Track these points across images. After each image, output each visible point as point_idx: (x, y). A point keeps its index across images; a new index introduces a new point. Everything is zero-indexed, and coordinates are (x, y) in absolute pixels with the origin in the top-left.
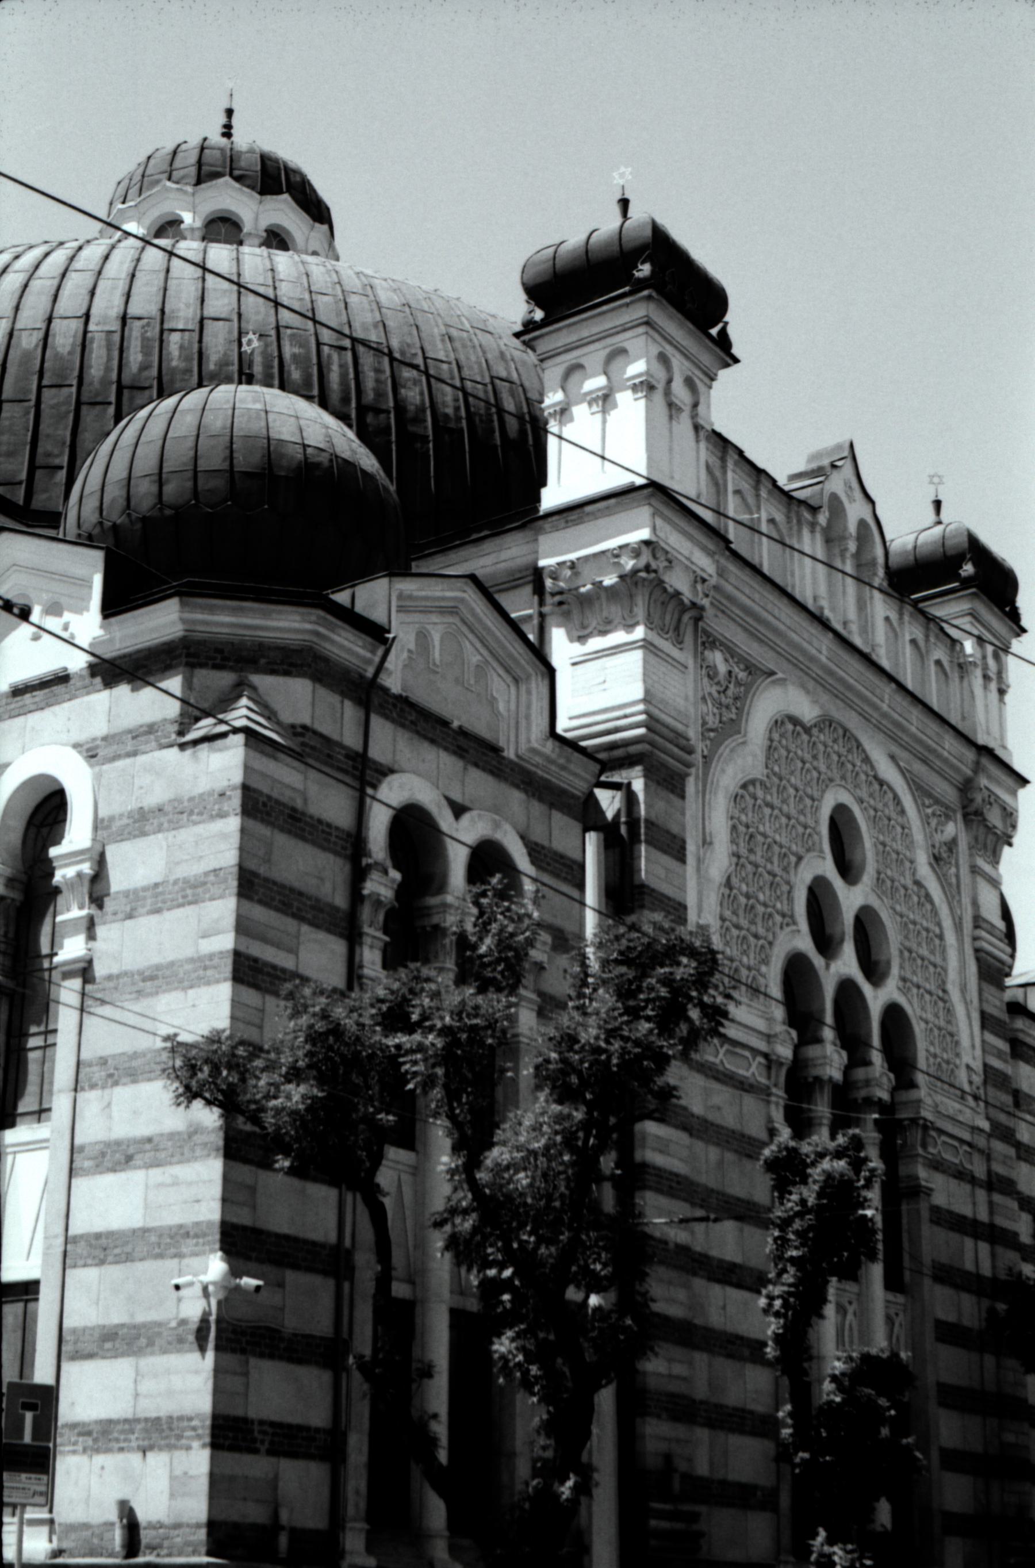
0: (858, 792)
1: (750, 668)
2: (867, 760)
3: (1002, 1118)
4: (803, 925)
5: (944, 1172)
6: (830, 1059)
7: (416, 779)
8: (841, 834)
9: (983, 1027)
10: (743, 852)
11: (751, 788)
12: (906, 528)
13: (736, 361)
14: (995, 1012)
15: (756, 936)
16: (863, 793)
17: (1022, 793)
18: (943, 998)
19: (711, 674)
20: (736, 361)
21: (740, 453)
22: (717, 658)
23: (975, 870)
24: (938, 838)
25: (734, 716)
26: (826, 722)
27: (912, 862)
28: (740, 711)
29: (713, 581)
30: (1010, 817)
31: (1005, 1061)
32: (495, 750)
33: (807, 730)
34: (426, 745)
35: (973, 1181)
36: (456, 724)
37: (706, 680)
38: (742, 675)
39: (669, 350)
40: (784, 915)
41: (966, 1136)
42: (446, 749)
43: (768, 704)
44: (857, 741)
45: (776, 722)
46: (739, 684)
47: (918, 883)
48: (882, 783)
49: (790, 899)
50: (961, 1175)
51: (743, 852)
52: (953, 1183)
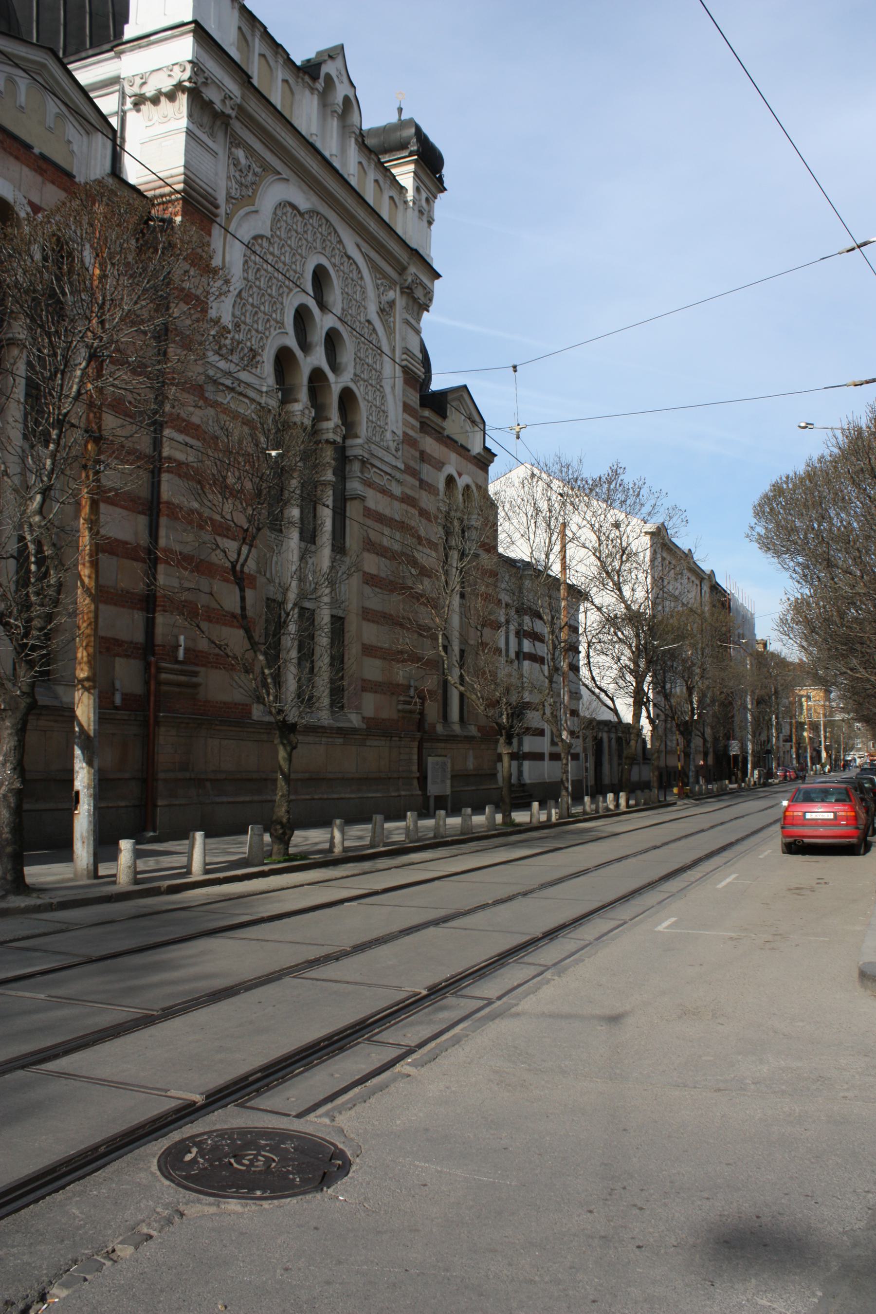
1: (267, 168)
2: (340, 242)
3: (412, 463)
5: (374, 489)
11: (260, 241)
16: (337, 260)
17: (436, 282)
18: (380, 389)
19: (236, 163)
22: (240, 154)
23: (407, 322)
24: (384, 299)
25: (250, 194)
26: (313, 212)
27: (365, 308)
28: (255, 192)
30: (429, 295)
31: (416, 432)
33: (301, 214)
35: (392, 496)
37: (232, 166)
38: (258, 170)
40: (277, 322)
41: (389, 470)
44: (334, 229)
45: (280, 204)
46: (255, 174)
47: (369, 322)
48: (349, 258)
49: (282, 314)
50: (384, 491)
52: (379, 495)
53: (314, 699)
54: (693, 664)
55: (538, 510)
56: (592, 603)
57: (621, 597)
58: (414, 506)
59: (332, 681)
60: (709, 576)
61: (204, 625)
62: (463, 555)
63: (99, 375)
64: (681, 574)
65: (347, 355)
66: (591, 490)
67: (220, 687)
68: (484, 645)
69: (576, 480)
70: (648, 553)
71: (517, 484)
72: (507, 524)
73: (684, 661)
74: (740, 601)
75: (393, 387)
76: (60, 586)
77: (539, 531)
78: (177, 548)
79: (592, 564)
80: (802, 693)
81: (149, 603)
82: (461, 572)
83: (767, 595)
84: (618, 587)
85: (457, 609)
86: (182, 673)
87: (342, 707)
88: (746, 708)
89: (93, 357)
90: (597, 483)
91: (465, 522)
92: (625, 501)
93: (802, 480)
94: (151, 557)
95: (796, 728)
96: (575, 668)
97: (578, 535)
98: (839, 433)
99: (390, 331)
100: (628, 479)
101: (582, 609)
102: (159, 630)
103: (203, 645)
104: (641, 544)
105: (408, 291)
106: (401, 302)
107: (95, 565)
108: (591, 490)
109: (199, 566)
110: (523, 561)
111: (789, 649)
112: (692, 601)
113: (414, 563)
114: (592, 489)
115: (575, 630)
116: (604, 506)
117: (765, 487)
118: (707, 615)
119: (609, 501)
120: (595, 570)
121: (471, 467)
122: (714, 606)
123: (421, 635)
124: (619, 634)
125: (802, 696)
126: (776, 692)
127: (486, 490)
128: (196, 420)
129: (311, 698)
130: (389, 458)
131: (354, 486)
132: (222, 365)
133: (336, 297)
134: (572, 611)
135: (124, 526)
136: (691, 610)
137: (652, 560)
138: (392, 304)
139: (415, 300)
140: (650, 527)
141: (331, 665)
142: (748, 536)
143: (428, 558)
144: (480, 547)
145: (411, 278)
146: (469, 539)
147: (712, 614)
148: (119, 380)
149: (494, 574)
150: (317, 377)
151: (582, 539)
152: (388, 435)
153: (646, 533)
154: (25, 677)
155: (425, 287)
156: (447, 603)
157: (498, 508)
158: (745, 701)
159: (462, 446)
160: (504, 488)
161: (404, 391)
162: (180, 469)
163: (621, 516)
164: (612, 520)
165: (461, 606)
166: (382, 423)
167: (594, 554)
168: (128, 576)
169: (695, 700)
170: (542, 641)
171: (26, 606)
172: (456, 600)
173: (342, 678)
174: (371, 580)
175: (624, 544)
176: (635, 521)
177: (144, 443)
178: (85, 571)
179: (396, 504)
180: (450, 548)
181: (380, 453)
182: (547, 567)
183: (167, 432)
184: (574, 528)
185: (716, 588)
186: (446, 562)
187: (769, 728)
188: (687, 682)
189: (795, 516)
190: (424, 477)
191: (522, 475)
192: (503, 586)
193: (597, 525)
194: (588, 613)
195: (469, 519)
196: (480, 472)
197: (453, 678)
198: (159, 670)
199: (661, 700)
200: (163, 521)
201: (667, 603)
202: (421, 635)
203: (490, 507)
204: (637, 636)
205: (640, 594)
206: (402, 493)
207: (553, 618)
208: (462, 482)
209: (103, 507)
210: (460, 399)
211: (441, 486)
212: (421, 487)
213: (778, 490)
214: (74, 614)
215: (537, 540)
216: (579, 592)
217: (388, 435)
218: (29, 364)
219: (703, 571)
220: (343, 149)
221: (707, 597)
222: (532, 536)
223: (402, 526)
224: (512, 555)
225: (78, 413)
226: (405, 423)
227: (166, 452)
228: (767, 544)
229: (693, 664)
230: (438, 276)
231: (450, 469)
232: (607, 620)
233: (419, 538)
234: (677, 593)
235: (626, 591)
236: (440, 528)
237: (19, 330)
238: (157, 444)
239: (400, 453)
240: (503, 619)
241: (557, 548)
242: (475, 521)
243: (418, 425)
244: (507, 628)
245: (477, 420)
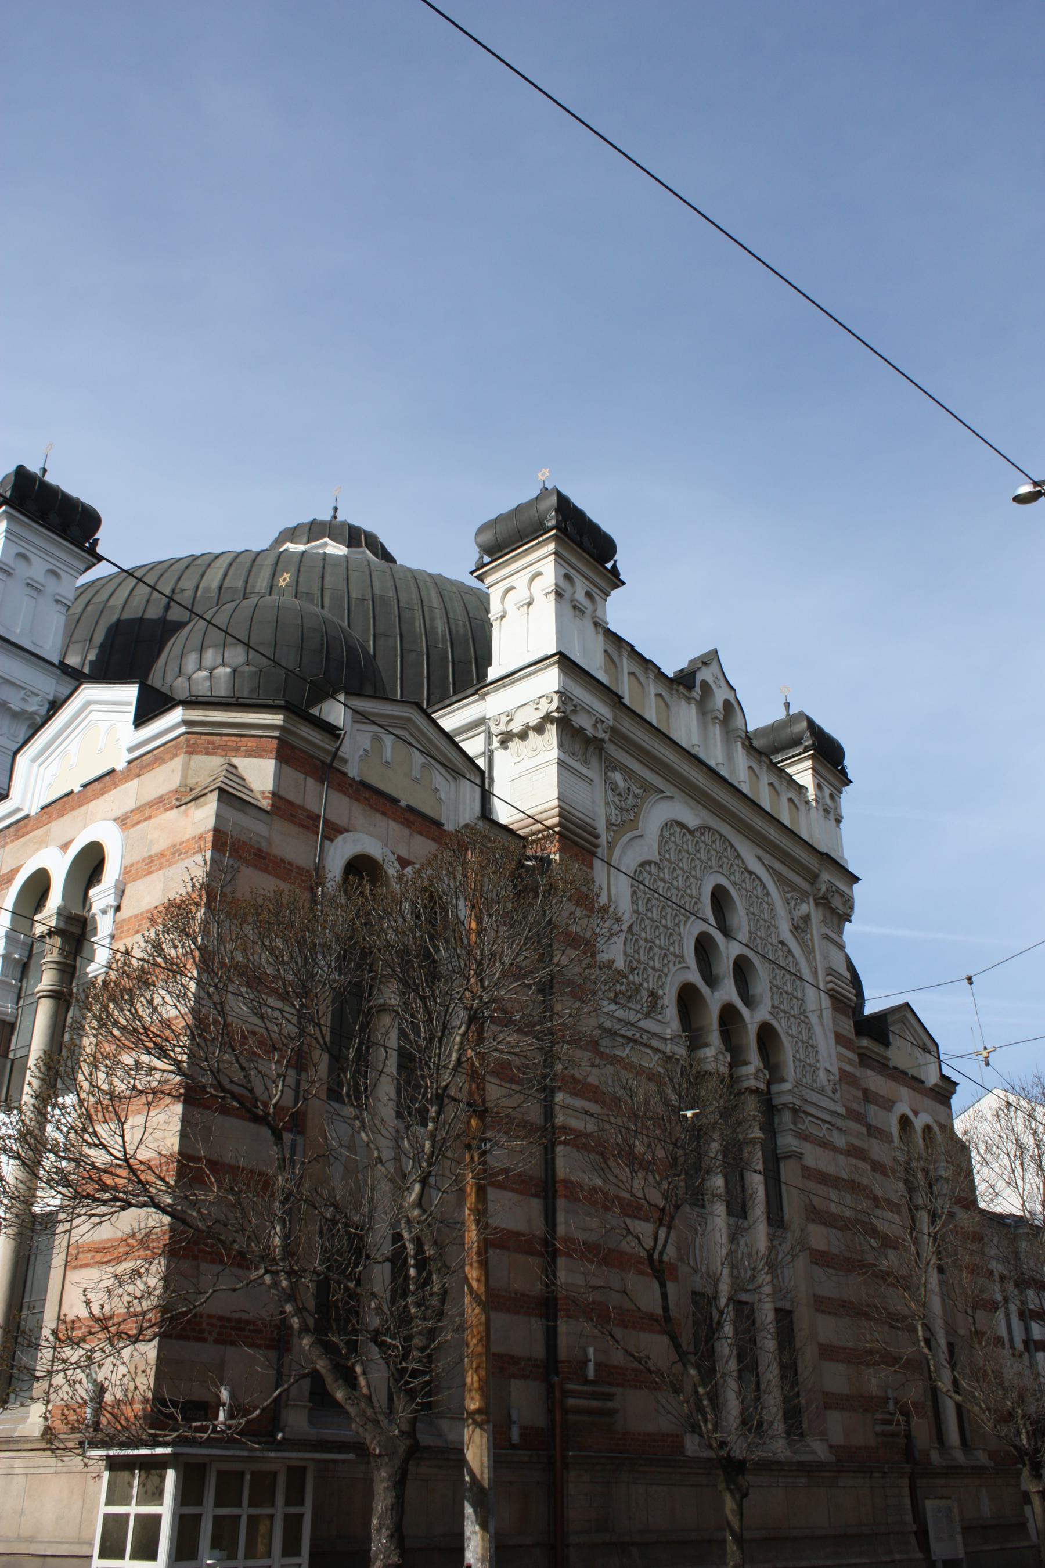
0: (732, 878)
1: (648, 788)
2: (739, 857)
3: (855, 1106)
5: (811, 1142)
7: (367, 838)
11: (648, 868)
13: (623, 583)
14: (845, 1033)
16: (737, 878)
17: (855, 887)
18: (803, 1018)
19: (614, 788)
20: (623, 583)
21: (632, 647)
22: (617, 777)
23: (827, 938)
26: (704, 828)
27: (776, 928)
28: (637, 816)
30: (849, 903)
31: (855, 1067)
32: (439, 824)
33: (691, 832)
34: (378, 815)
35: (834, 1149)
36: (403, 803)
37: (609, 792)
38: (637, 791)
39: (572, 572)
40: (676, 956)
41: (828, 1118)
42: (394, 820)
43: (659, 814)
44: (730, 843)
45: (666, 824)
46: (636, 796)
47: (782, 943)
48: (751, 873)
49: (681, 945)
50: (825, 1144)
52: (819, 1150)
53: (765, 1426)
58: (864, 1160)
59: (786, 1399)
61: (618, 1332)
62: (934, 1217)
63: (481, 1040)
65: (762, 984)
67: (644, 1413)
68: (979, 1334)
71: (990, 1118)
72: (985, 1170)
75: (820, 1017)
76: (445, 1293)
77: (1028, 1175)
78: (580, 1236)
81: (548, 1307)
82: (935, 1239)
86: (594, 1396)
89: (474, 1018)
91: (932, 1173)
94: (548, 1249)
99: (808, 950)
102: (562, 1341)
103: (618, 1358)
105: (823, 902)
107: (484, 1264)
109: (610, 1258)
110: (1013, 1215)
113: (873, 1232)
121: (930, 1103)
128: (592, 1080)
131: (787, 1141)
132: (620, 1014)
133: (740, 919)
135: (514, 1213)
138: (806, 919)
139: (833, 911)
141: (783, 1377)
143: (890, 1223)
144: (955, 1203)
145: (825, 886)
146: (940, 1194)
148: (504, 1042)
149: (978, 1238)
150: (729, 1015)
152: (822, 1074)
154: (404, 1411)
155: (842, 894)
157: (970, 1152)
159: (914, 1078)
161: (834, 1019)
162: (579, 1141)
165: (942, 1283)
166: (812, 1061)
168: (522, 1275)
171: (404, 1319)
172: (934, 1278)
173: (798, 1395)
174: (820, 1258)
177: (534, 1113)
178: (473, 1274)
179: (842, 1159)
181: (815, 1097)
183: (559, 1097)
190: (872, 1121)
192: (994, 1251)
195: (936, 1169)
196: (941, 1108)
197: (944, 1384)
198: (565, 1394)
200: (561, 1203)
202: (892, 1327)
203: (960, 1150)
206: (847, 1143)
208: (919, 1122)
209: (491, 1193)
210: (903, 1021)
211: (895, 1129)
212: (869, 1134)
214: (461, 1328)
215: (1028, 1186)
217: (822, 1074)
218: (402, 1033)
220: (730, 756)
222: (1020, 1183)
223: (853, 1187)
224: (998, 1210)
225: (459, 1086)
226: (840, 1057)
227: (560, 1120)
230: (857, 879)
231: (903, 1108)
233: (876, 1199)
236: (901, 1185)
237: (390, 994)
238: (549, 1113)
239: (838, 1095)
240: (999, 1297)
242: (944, 1170)
243: (856, 1058)
244: (1007, 1308)
245: (928, 1045)
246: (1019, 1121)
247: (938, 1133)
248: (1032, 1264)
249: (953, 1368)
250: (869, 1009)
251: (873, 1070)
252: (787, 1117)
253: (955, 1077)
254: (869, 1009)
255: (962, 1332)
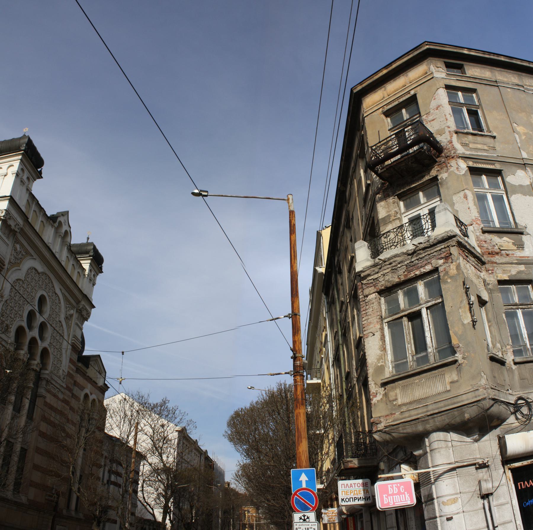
2: (53, 287)
3: (70, 385)
4: (25, 319)
6: (23, 353)
8: (42, 300)
9: (70, 362)
10: (12, 295)
12: (77, 239)
13: (42, 178)
15: (11, 317)
16: (50, 294)
18: (60, 350)
20: (42, 178)
24: (68, 313)
26: (44, 273)
29: (21, 226)
33: (39, 273)
41: (59, 387)
47: (60, 322)
48: (56, 294)
50: (55, 396)
51: (12, 295)
52: (52, 397)
53: (6, 486)
54: (194, 495)
55: (126, 415)
56: (147, 461)
57: (162, 459)
58: (68, 405)
59: (16, 479)
60: (205, 452)
62: (87, 431)
64: (192, 451)
66: (152, 409)
68: (92, 475)
69: (145, 404)
70: (176, 440)
71: (117, 402)
72: (110, 420)
73: (190, 492)
74: (219, 465)
75: (66, 351)
77: (125, 425)
79: (149, 443)
80: (246, 509)
82: (86, 438)
83: (230, 462)
84: (161, 455)
85: (81, 456)
87: (19, 492)
88: (218, 517)
90: (156, 406)
91: (91, 416)
92: (167, 416)
93: (248, 411)
95: (242, 526)
96: (136, 492)
97: (144, 429)
98: (264, 393)
100: (170, 405)
101: (142, 463)
104: (173, 436)
105: (79, 312)
106: (75, 316)
108: (152, 409)
110: (116, 437)
111: (239, 487)
112: (196, 464)
113: (64, 430)
114: (153, 408)
115: (138, 473)
116: (158, 416)
117: (232, 413)
118: (202, 471)
119: (160, 414)
120: (150, 446)
121: (97, 391)
122: (206, 467)
123: (62, 465)
124: (159, 477)
125: (246, 511)
126: (233, 508)
127: (103, 403)
129: (4, 484)
130: (59, 382)
131: (42, 391)
134: (137, 464)
136: (195, 469)
137: (178, 444)
138: (71, 316)
139: (82, 316)
140: (178, 428)
141: (17, 471)
142: (224, 436)
143: (71, 429)
144: (97, 428)
145: (82, 306)
146: (91, 424)
147: (205, 471)
151: (146, 431)
152: (61, 371)
153: (177, 431)
155: (87, 311)
156: (77, 451)
157: (107, 412)
158: (219, 514)
159: (94, 381)
160: (111, 403)
161: (71, 353)
163: (165, 422)
164: (160, 424)
165: (84, 454)
166: (59, 366)
167: (151, 438)
169: (194, 512)
170: (121, 477)
172: (81, 452)
173: (21, 478)
174: (42, 435)
175: (165, 435)
176: (171, 425)
179: (60, 402)
180: (82, 426)
181: (56, 378)
182: (127, 442)
184: (142, 425)
185: (207, 458)
186: (79, 433)
187: (229, 526)
188: (190, 503)
189: (243, 427)
190: (74, 392)
191: (120, 398)
192: (105, 448)
193: (153, 426)
194: (145, 466)
195: (93, 415)
199: (177, 511)
201: (184, 465)
202: (62, 465)
204: (168, 479)
205: (171, 459)
206: (63, 398)
207: (127, 466)
208: (91, 397)
210: (96, 361)
212: (72, 397)
213: (237, 414)
215: (124, 429)
216: (142, 455)
219: (202, 450)
220: (61, 250)
221: (203, 462)
222: (121, 427)
223: (61, 413)
224: (111, 434)
228: (231, 439)
229: (194, 495)
231: (87, 391)
232: (154, 470)
233: (68, 419)
234: (189, 460)
235: (164, 457)
236: (78, 417)
239: (65, 380)
240: (103, 464)
241: (133, 434)
243: (75, 369)
244: (105, 468)
245: (102, 371)
246: (127, 407)
247: (97, 402)
248: (118, 455)
249: (79, 484)
250: (85, 353)
251: (80, 375)
252: (44, 383)
253: (109, 385)
254: (85, 353)
255: (86, 472)
